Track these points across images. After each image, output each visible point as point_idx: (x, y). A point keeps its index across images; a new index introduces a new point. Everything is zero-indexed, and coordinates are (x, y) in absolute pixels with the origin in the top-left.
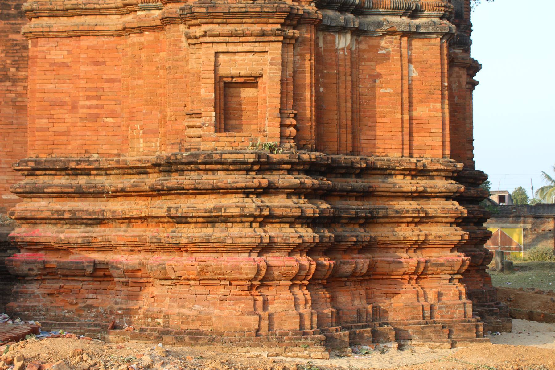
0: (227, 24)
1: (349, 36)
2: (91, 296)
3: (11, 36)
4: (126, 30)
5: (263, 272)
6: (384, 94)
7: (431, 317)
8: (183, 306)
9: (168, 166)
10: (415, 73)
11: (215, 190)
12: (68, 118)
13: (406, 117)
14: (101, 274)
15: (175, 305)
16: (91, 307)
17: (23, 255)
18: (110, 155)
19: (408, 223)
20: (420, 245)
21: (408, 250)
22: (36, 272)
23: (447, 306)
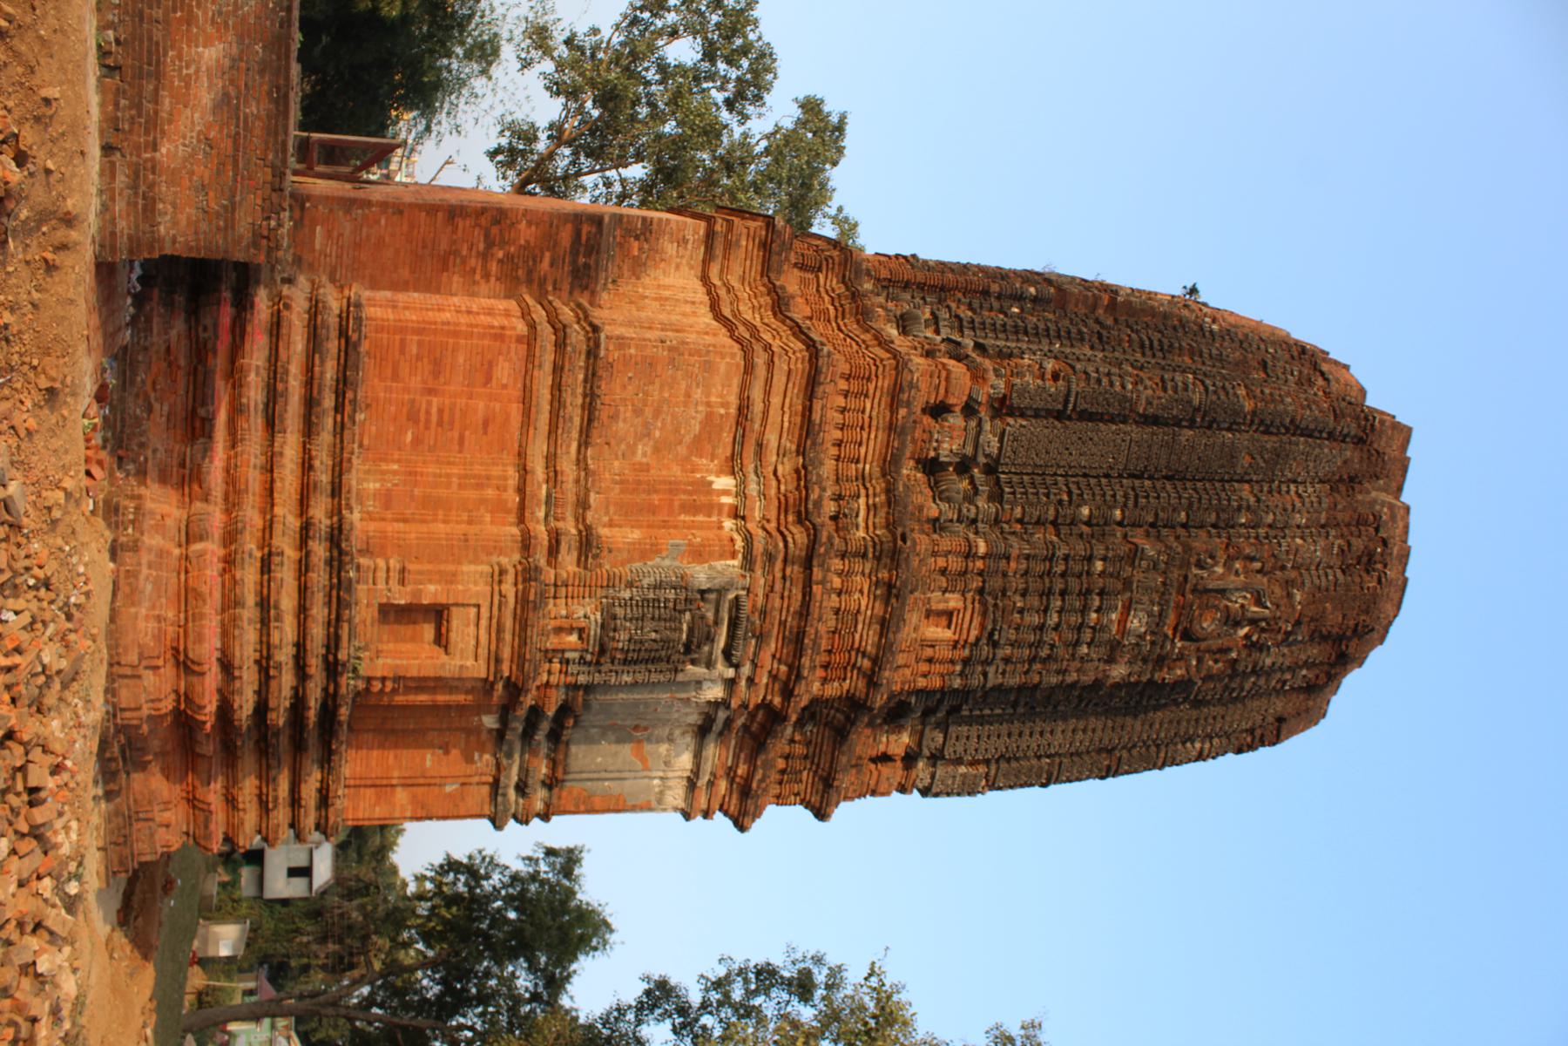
1: (496, 726)
2: (166, 408)
3: (547, 255)
4: (524, 471)
5: (196, 668)
6: (424, 759)
7: (138, 820)
8: (150, 567)
9: (336, 537)
10: (448, 789)
11: (302, 610)
12: (416, 382)
13: (394, 782)
14: (196, 427)
15: (152, 557)
16: (150, 410)
17: (226, 314)
18: (362, 435)
19: (260, 788)
20: (231, 801)
21: (227, 788)
22: (202, 335)
23: (152, 835)
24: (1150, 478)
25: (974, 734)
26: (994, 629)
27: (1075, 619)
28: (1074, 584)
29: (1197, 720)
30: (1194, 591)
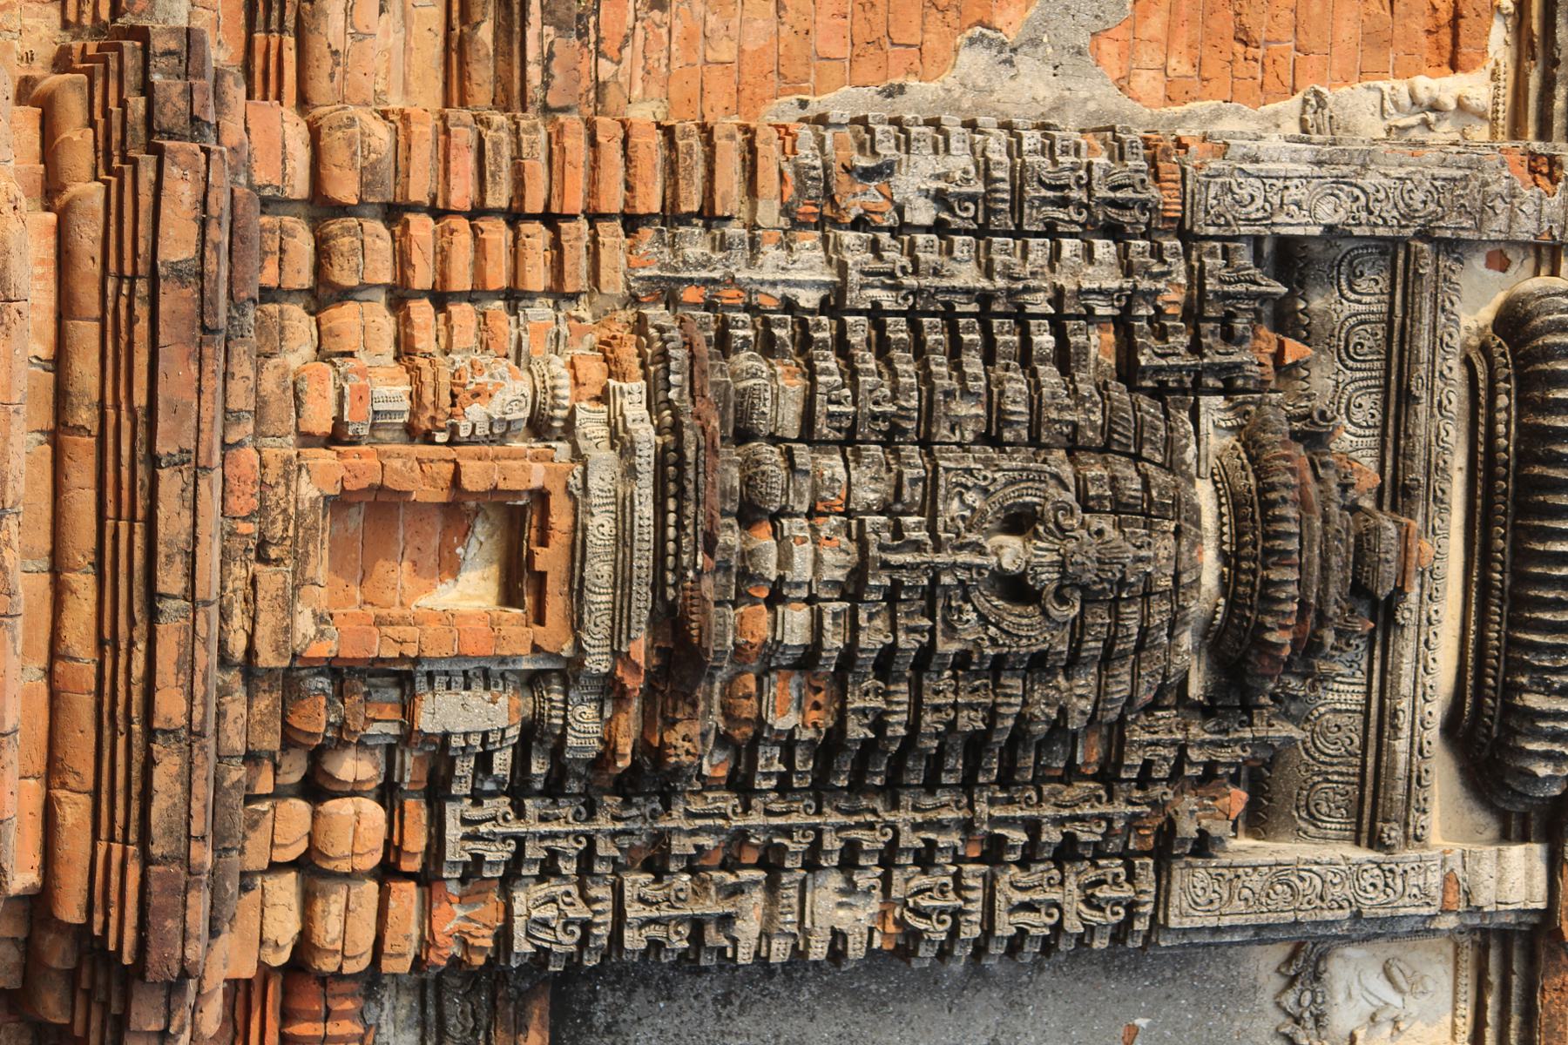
0: (58, 434)
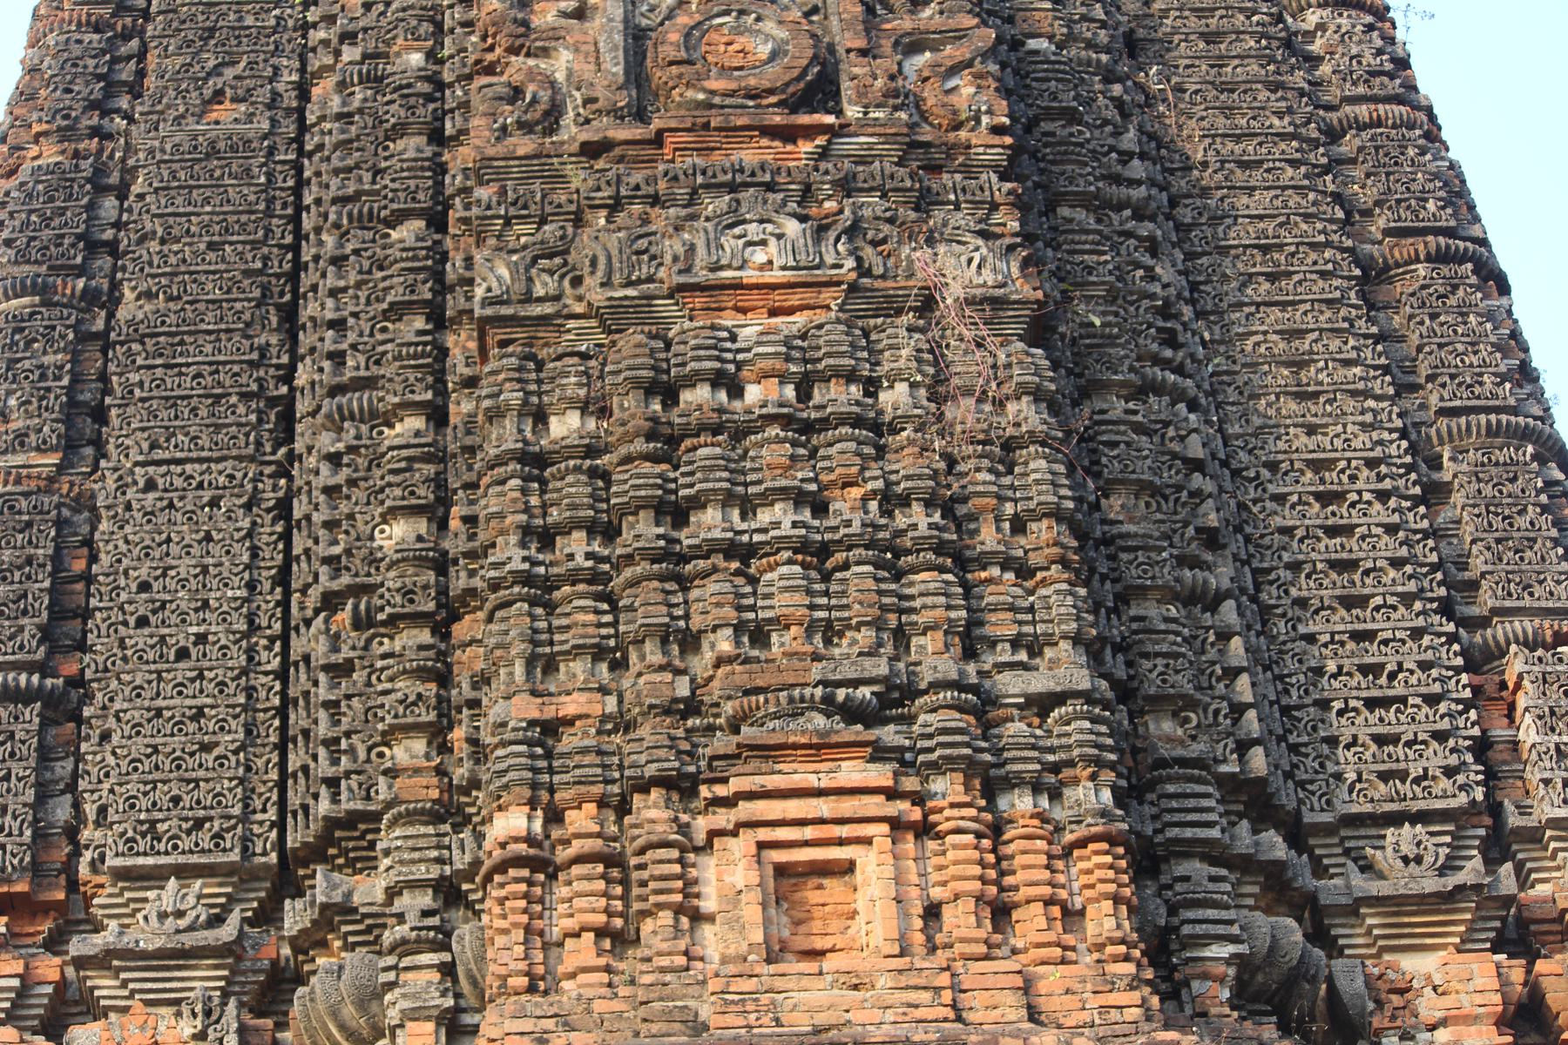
24: (288, 376)
25: (1366, 724)
26: (829, 706)
27: (770, 453)
28: (635, 480)
29: (1211, 38)
30: (641, 116)
